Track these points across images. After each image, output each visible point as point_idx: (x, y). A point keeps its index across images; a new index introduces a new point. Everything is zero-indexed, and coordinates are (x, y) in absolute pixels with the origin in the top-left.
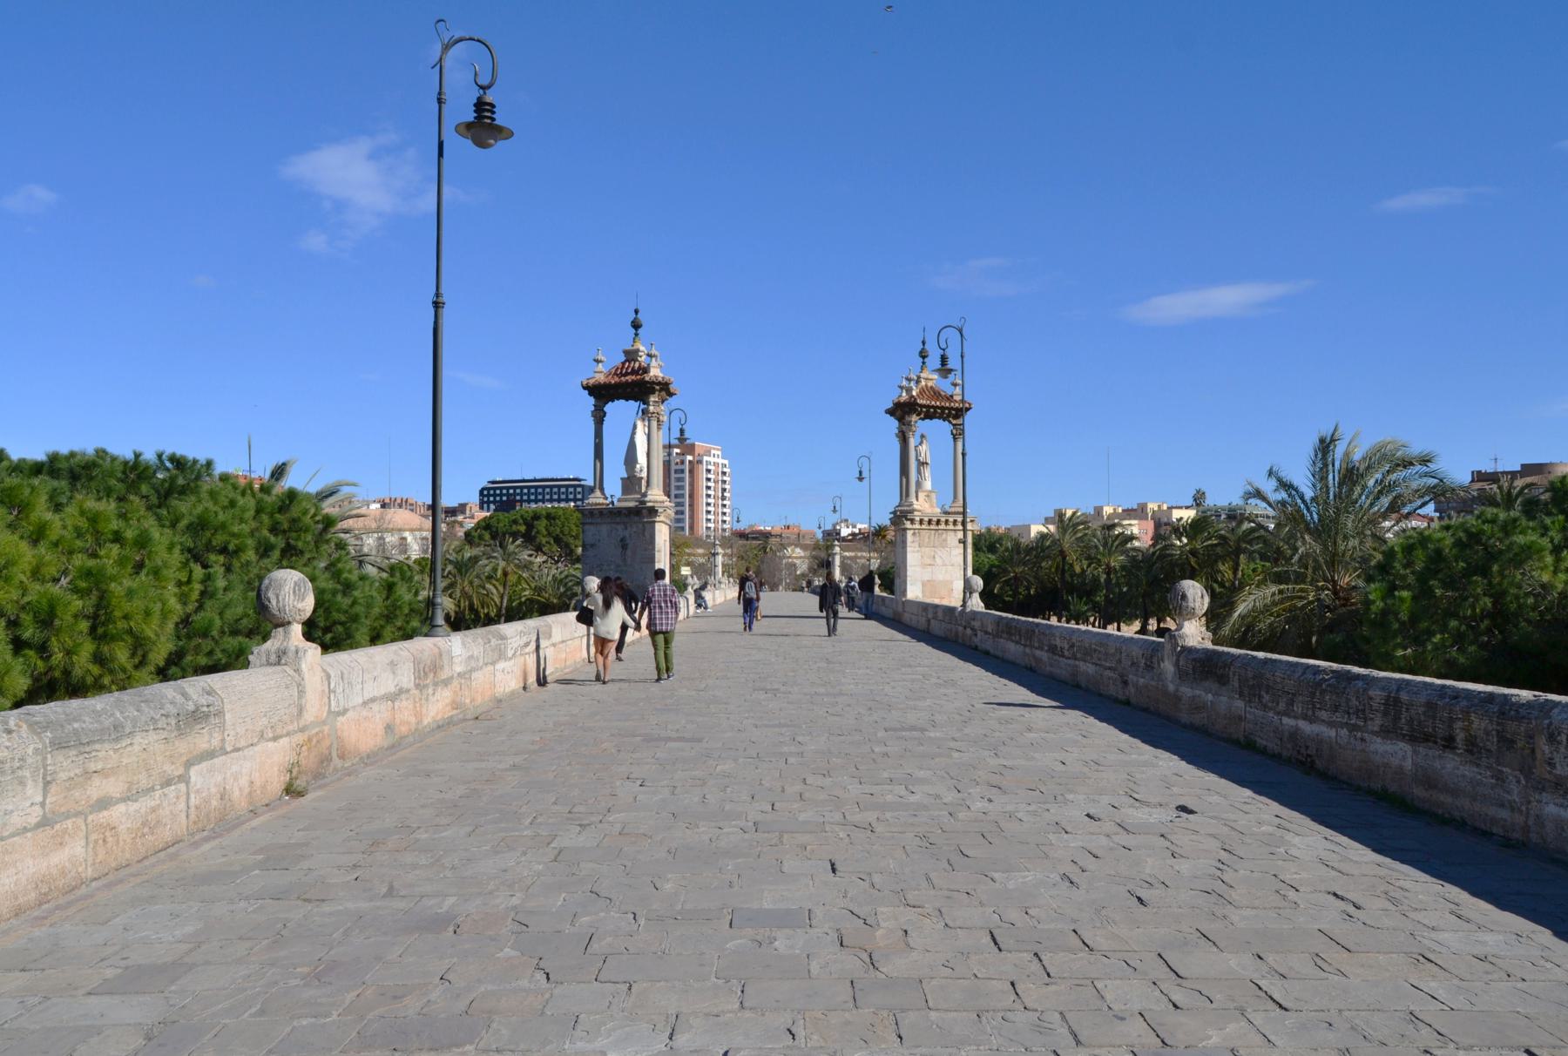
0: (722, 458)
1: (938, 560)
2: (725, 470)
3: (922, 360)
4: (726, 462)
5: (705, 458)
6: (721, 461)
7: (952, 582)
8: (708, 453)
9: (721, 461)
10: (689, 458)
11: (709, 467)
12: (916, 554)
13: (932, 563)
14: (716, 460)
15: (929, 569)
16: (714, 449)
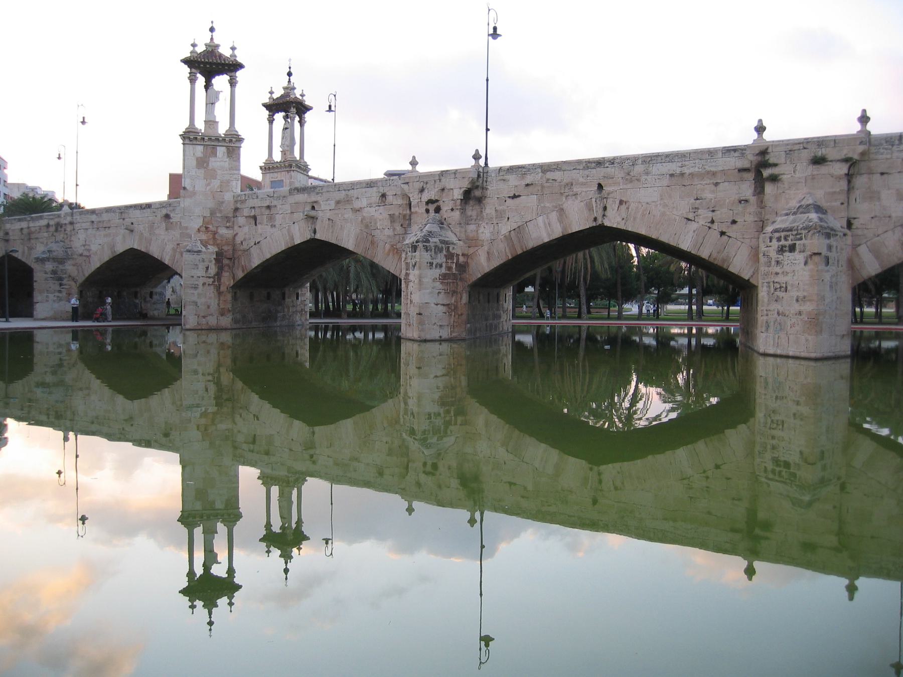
3: (210, 34)
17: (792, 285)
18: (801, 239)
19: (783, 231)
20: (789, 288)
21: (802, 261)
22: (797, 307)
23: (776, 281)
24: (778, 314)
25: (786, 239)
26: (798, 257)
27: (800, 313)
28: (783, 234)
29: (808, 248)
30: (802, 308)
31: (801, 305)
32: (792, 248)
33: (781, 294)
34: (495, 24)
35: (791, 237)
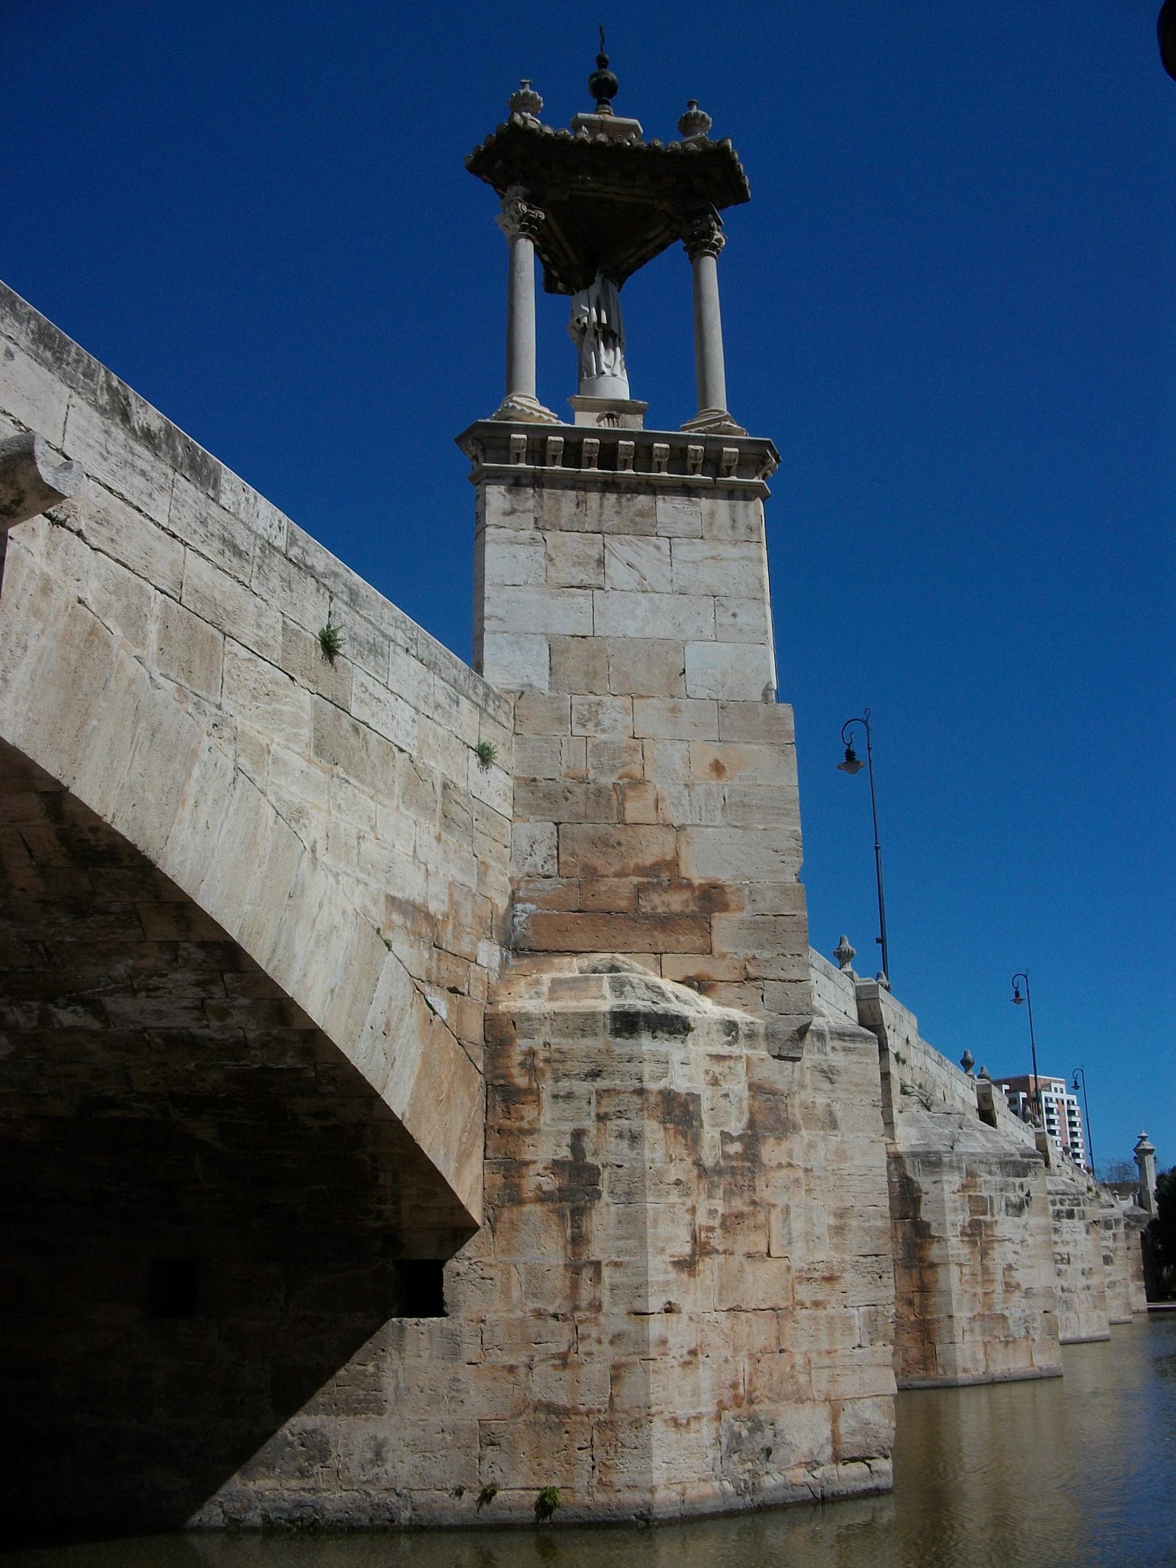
0: (1067, 1093)
1: (617, 572)
2: (1073, 1108)
4: (1074, 1098)
5: (1044, 1094)
6: (1066, 1097)
7: (680, 648)
8: (1048, 1087)
9: (1066, 1097)
10: (1023, 1095)
11: (1051, 1105)
12: (523, 552)
13: (600, 580)
14: (1059, 1095)
15: (582, 599)
16: (1056, 1082)
17: (1075, 1256)
18: (1079, 1205)
19: (1057, 1194)
20: (1072, 1259)
21: (1083, 1229)
22: (1083, 1281)
23: (1056, 1250)
24: (1063, 1290)
25: (1062, 1204)
26: (1078, 1224)
27: (1088, 1288)
28: (1058, 1197)
29: (1088, 1215)
30: (1089, 1282)
31: (1087, 1278)
32: (1070, 1215)
33: (1063, 1267)
34: (849, 745)
35: (1068, 1202)
